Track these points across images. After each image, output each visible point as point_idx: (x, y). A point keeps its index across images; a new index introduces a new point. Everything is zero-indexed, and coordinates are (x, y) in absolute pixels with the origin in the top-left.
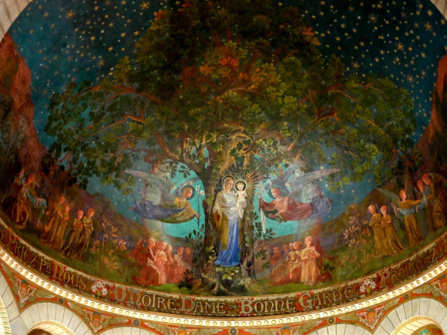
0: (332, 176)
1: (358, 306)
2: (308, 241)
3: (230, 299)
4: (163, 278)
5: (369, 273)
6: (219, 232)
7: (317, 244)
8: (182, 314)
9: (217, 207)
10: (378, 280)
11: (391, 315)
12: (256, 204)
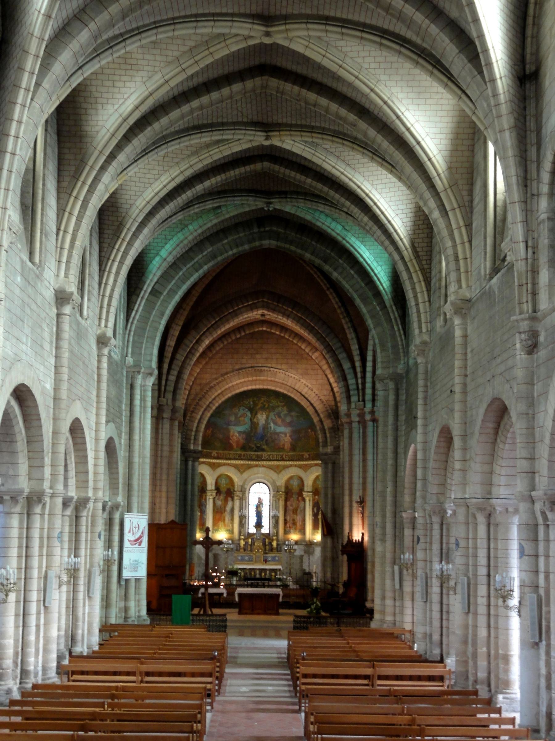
0: (297, 416)
1: (302, 463)
2: (288, 435)
3: (259, 453)
4: (235, 447)
5: (307, 451)
6: (256, 428)
7: (291, 436)
8: (242, 460)
9: (255, 420)
10: (309, 455)
11: (312, 468)
12: (270, 421)
